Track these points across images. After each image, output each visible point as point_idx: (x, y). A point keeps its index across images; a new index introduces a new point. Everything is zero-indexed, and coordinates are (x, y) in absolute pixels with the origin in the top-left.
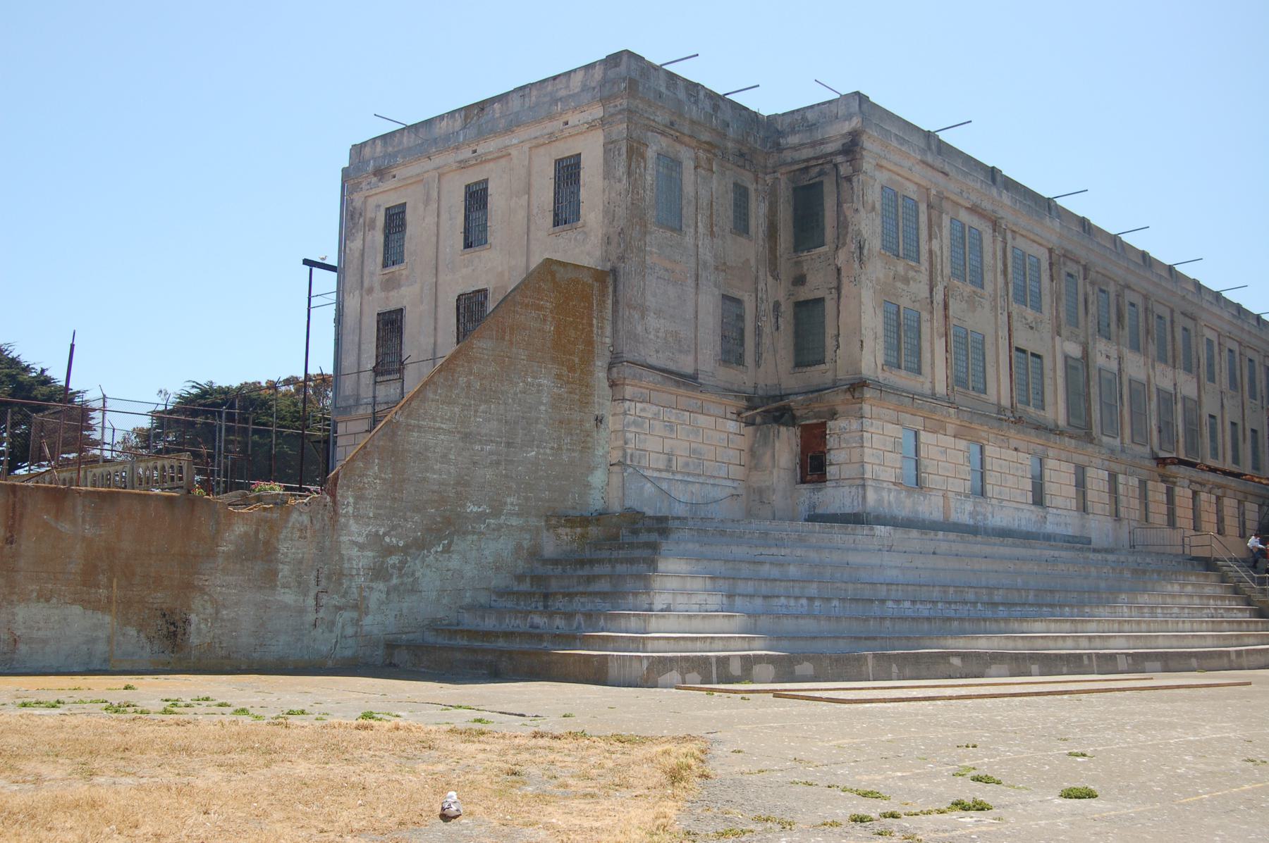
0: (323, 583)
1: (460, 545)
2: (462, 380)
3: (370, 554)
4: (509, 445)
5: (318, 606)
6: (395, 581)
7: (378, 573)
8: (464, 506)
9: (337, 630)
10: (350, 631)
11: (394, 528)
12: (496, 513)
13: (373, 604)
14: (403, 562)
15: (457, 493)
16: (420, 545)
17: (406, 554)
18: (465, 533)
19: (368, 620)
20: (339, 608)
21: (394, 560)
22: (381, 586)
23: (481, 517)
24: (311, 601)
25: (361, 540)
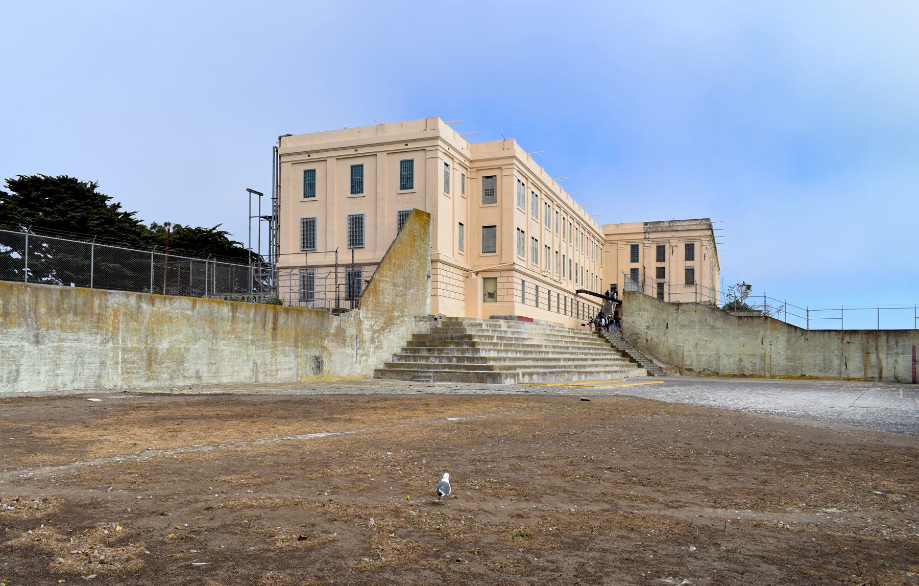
0: (358, 345)
1: (394, 328)
2: (393, 260)
3: (370, 333)
4: (406, 288)
5: (357, 354)
6: (376, 344)
7: (372, 341)
8: (394, 313)
9: (362, 364)
10: (365, 364)
11: (376, 323)
12: (402, 316)
13: (371, 354)
14: (379, 336)
15: (392, 308)
16: (383, 329)
17: (380, 333)
18: (394, 324)
19: (369, 360)
20: (362, 355)
21: (376, 335)
22: (373, 346)
23: (398, 317)
24: (355, 353)
25: (368, 327)
